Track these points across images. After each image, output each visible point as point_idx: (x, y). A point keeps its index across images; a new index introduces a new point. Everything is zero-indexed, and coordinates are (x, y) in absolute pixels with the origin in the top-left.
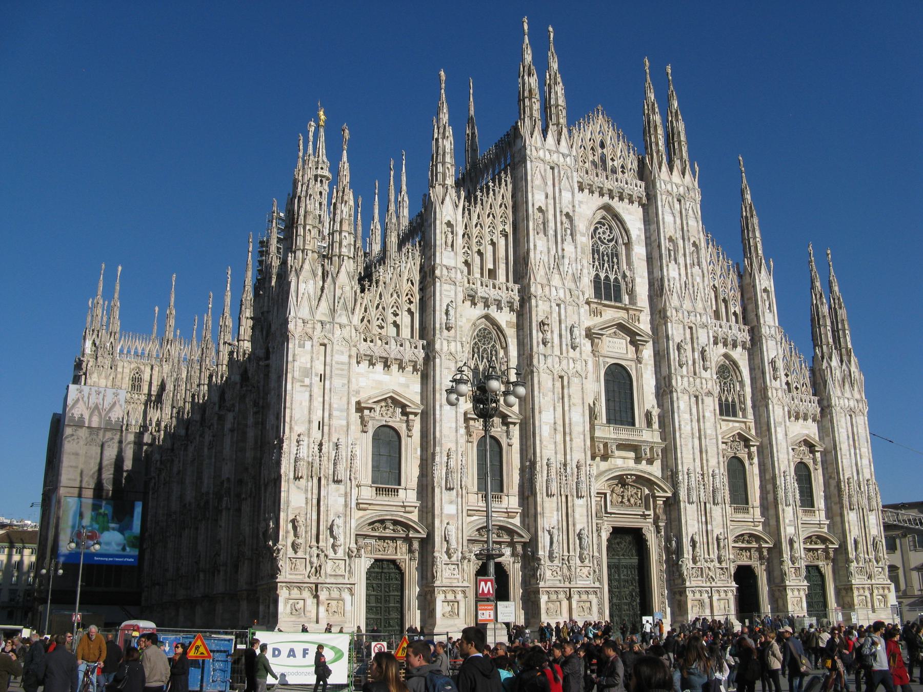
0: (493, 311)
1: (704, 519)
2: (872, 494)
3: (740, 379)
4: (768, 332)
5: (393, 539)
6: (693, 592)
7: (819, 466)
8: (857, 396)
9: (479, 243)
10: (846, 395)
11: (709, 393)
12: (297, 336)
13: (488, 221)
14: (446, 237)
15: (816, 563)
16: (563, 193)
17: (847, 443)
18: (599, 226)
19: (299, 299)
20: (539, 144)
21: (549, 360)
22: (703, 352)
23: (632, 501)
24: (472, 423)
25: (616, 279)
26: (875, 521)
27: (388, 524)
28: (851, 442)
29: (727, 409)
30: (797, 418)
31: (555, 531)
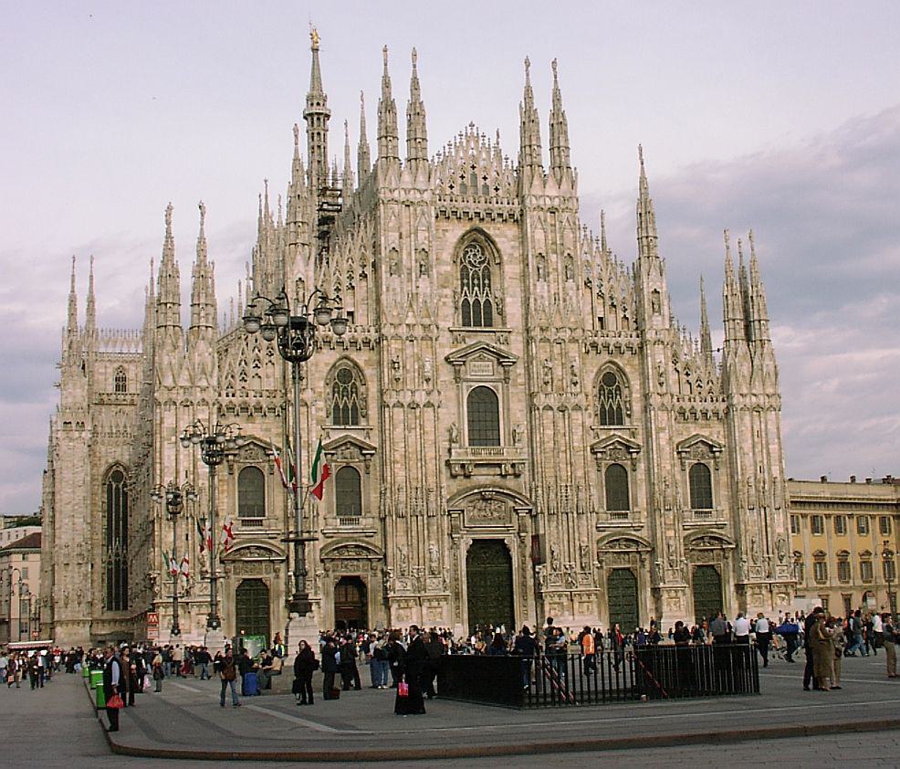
0: (354, 355)
11: (577, 408)
13: (345, 266)
23: (496, 514)
27: (253, 550)
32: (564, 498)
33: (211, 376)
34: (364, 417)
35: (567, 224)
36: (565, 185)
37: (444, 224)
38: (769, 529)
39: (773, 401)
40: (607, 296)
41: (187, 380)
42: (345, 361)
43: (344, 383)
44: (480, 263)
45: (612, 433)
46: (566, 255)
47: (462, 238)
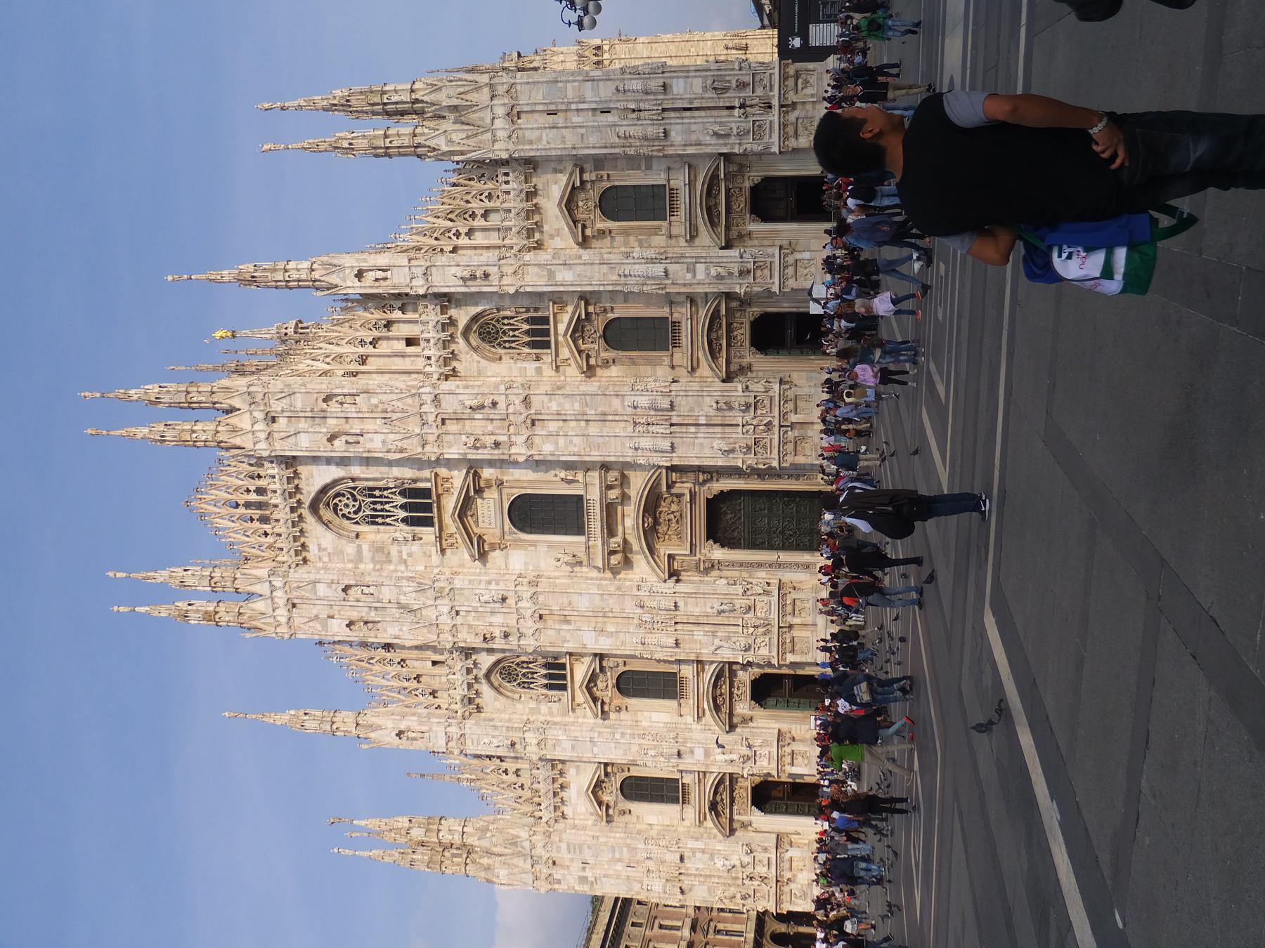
1: (692, 429)
5: (732, 791)
7: (604, 173)
11: (526, 401)
12: (549, 887)
13: (377, 668)
14: (415, 739)
20: (271, 620)
21: (523, 630)
23: (674, 507)
24: (606, 708)
26: (681, 81)
28: (559, 119)
29: (540, 338)
30: (537, 209)
31: (717, 642)
32: (651, 428)
33: (517, 837)
34: (556, 658)
35: (284, 401)
36: (236, 403)
37: (313, 547)
38: (695, 105)
39: (501, 90)
40: (376, 333)
42: (492, 679)
44: (355, 500)
45: (561, 339)
46: (324, 406)
47: (326, 524)
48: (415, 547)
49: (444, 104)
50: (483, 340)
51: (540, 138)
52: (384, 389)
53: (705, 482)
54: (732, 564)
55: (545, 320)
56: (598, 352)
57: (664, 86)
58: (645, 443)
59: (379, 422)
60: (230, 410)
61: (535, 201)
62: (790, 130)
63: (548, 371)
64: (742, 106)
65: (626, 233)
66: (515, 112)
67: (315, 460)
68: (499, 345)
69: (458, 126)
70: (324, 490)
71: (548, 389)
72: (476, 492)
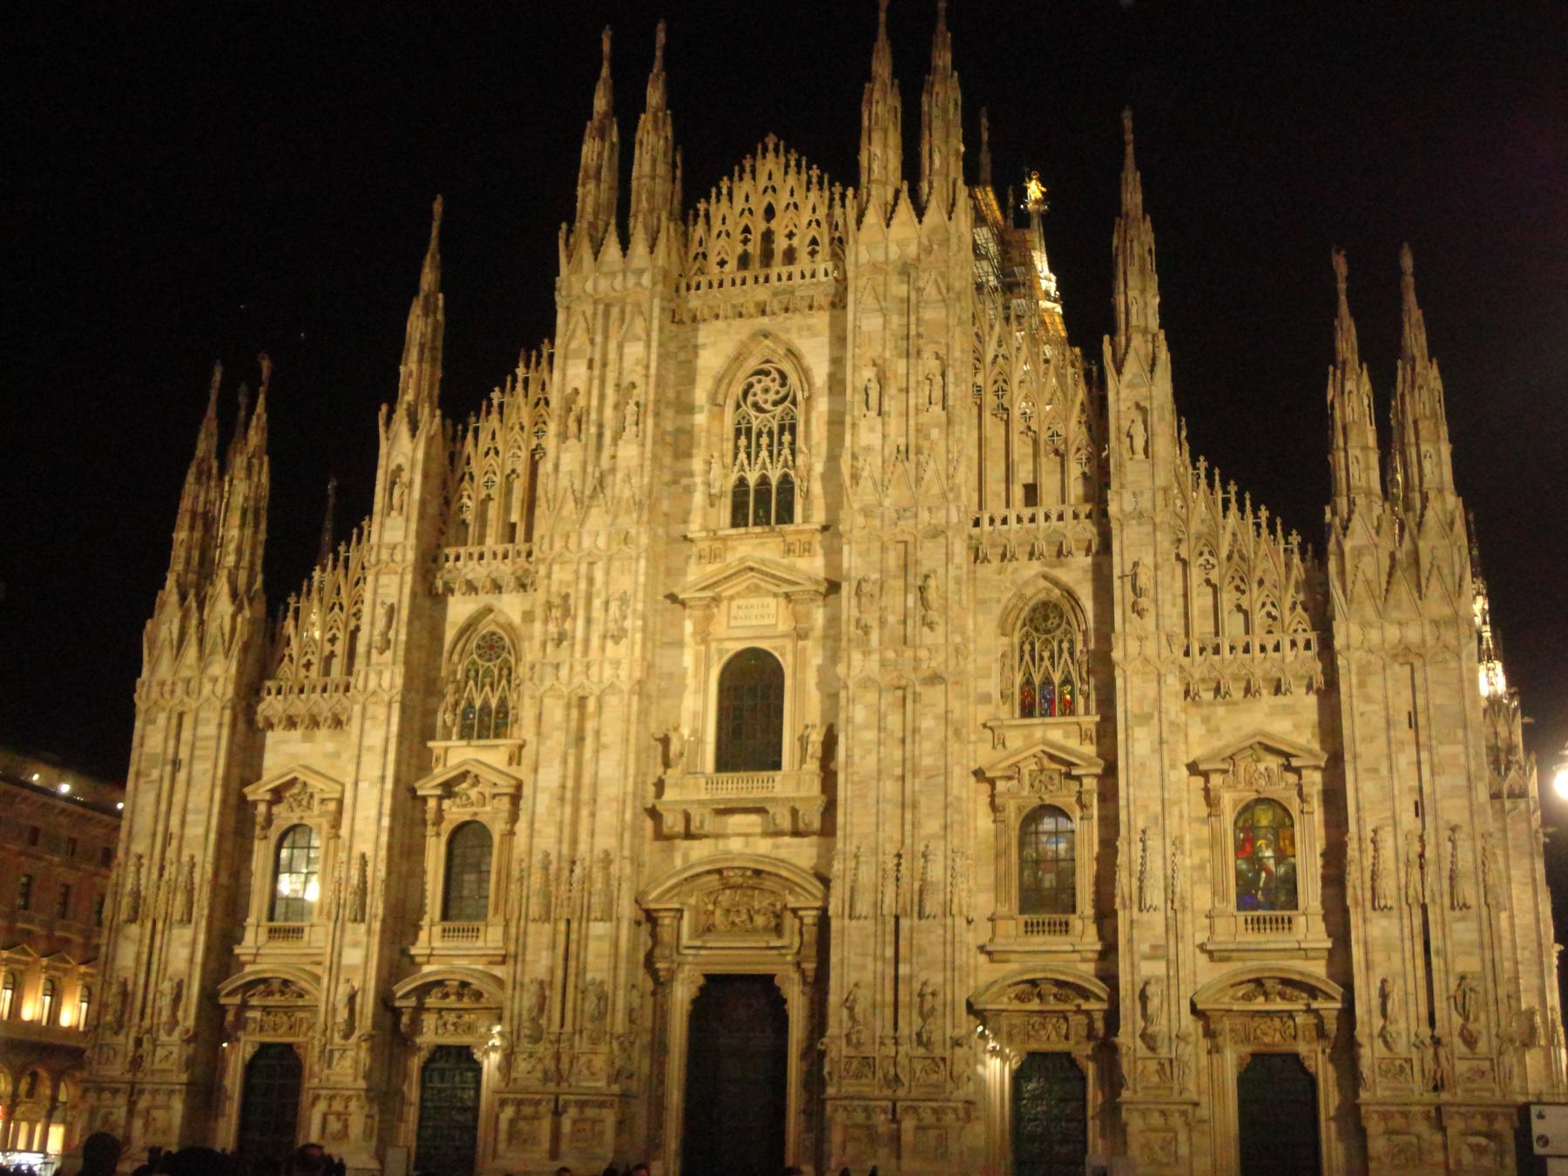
1: (889, 952)
2: (1466, 860)
3: (1083, 627)
4: (1128, 507)
6: (845, 1108)
8: (1436, 606)
9: (489, 484)
10: (1395, 615)
11: (935, 679)
15: (1286, 1048)
16: (627, 350)
17: (1382, 739)
18: (754, 379)
19: (156, 653)
22: (922, 589)
23: (760, 921)
25: (786, 481)
26: (1475, 936)
28: (1403, 733)
36: (934, 214)
38: (1434, 960)
39: (1449, 636)
40: (1044, 436)
41: (190, 667)
43: (490, 660)
45: (1038, 734)
47: (738, 358)
48: (699, 498)
49: (1421, 544)
50: (1034, 610)
51: (1368, 699)
52: (955, 449)
53: (803, 973)
54: (661, 1015)
55: (1069, 708)
56: (1015, 796)
57: (1468, 908)
58: (866, 874)
59: (902, 441)
60: (920, 211)
61: (1264, 692)
62: (1398, 1122)
63: (983, 713)
64: (1437, 1042)
65: (1214, 842)
66: (1412, 659)
67: (839, 340)
68: (1027, 635)
69: (1386, 563)
70: (792, 353)
71: (956, 715)
72: (787, 596)
